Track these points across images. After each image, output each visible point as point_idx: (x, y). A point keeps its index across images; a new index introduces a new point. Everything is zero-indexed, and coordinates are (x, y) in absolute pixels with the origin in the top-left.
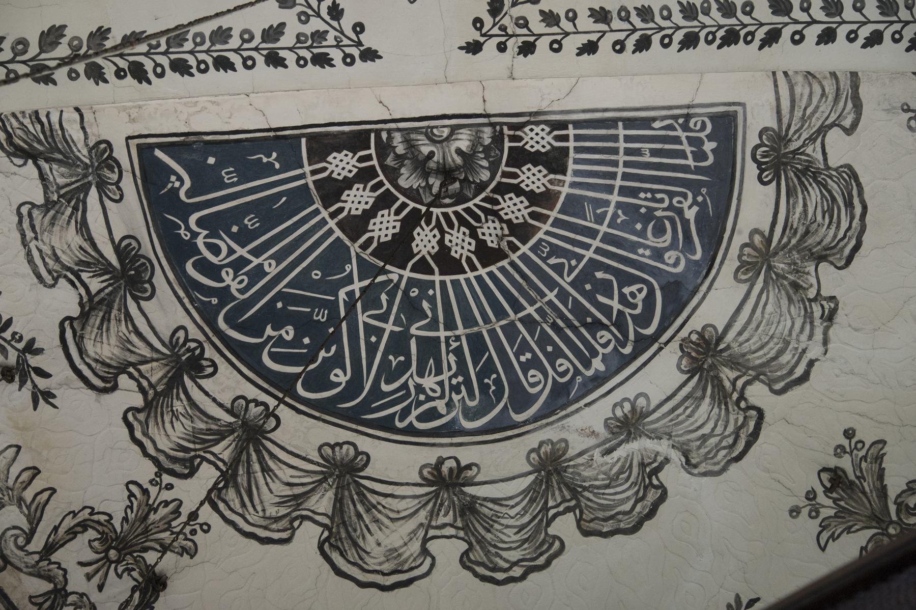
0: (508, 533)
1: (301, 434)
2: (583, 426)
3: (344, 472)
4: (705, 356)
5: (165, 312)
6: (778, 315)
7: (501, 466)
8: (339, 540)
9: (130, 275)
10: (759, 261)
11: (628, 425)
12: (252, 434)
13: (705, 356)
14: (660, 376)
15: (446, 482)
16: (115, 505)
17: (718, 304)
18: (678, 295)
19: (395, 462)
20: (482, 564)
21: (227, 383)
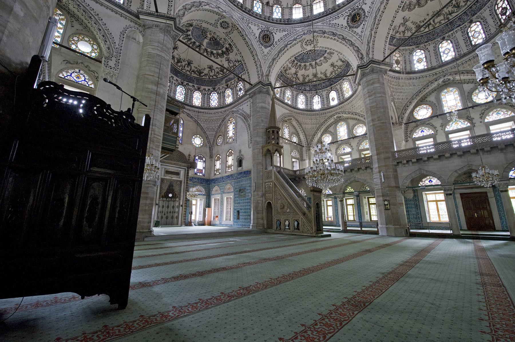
0: (314, 66)
1: (303, 64)
2: (318, 61)
3: (305, 65)
4: (325, 58)
5: (296, 62)
6: (329, 56)
7: (314, 63)
8: (305, 69)
9: (294, 61)
10: (328, 53)
11: (321, 61)
12: (300, 65)
13: (325, 58)
14: (322, 58)
15: (310, 64)
16: (295, 72)
17: (326, 55)
18: (323, 55)
19: (308, 64)
20: (313, 68)
21: (299, 63)
